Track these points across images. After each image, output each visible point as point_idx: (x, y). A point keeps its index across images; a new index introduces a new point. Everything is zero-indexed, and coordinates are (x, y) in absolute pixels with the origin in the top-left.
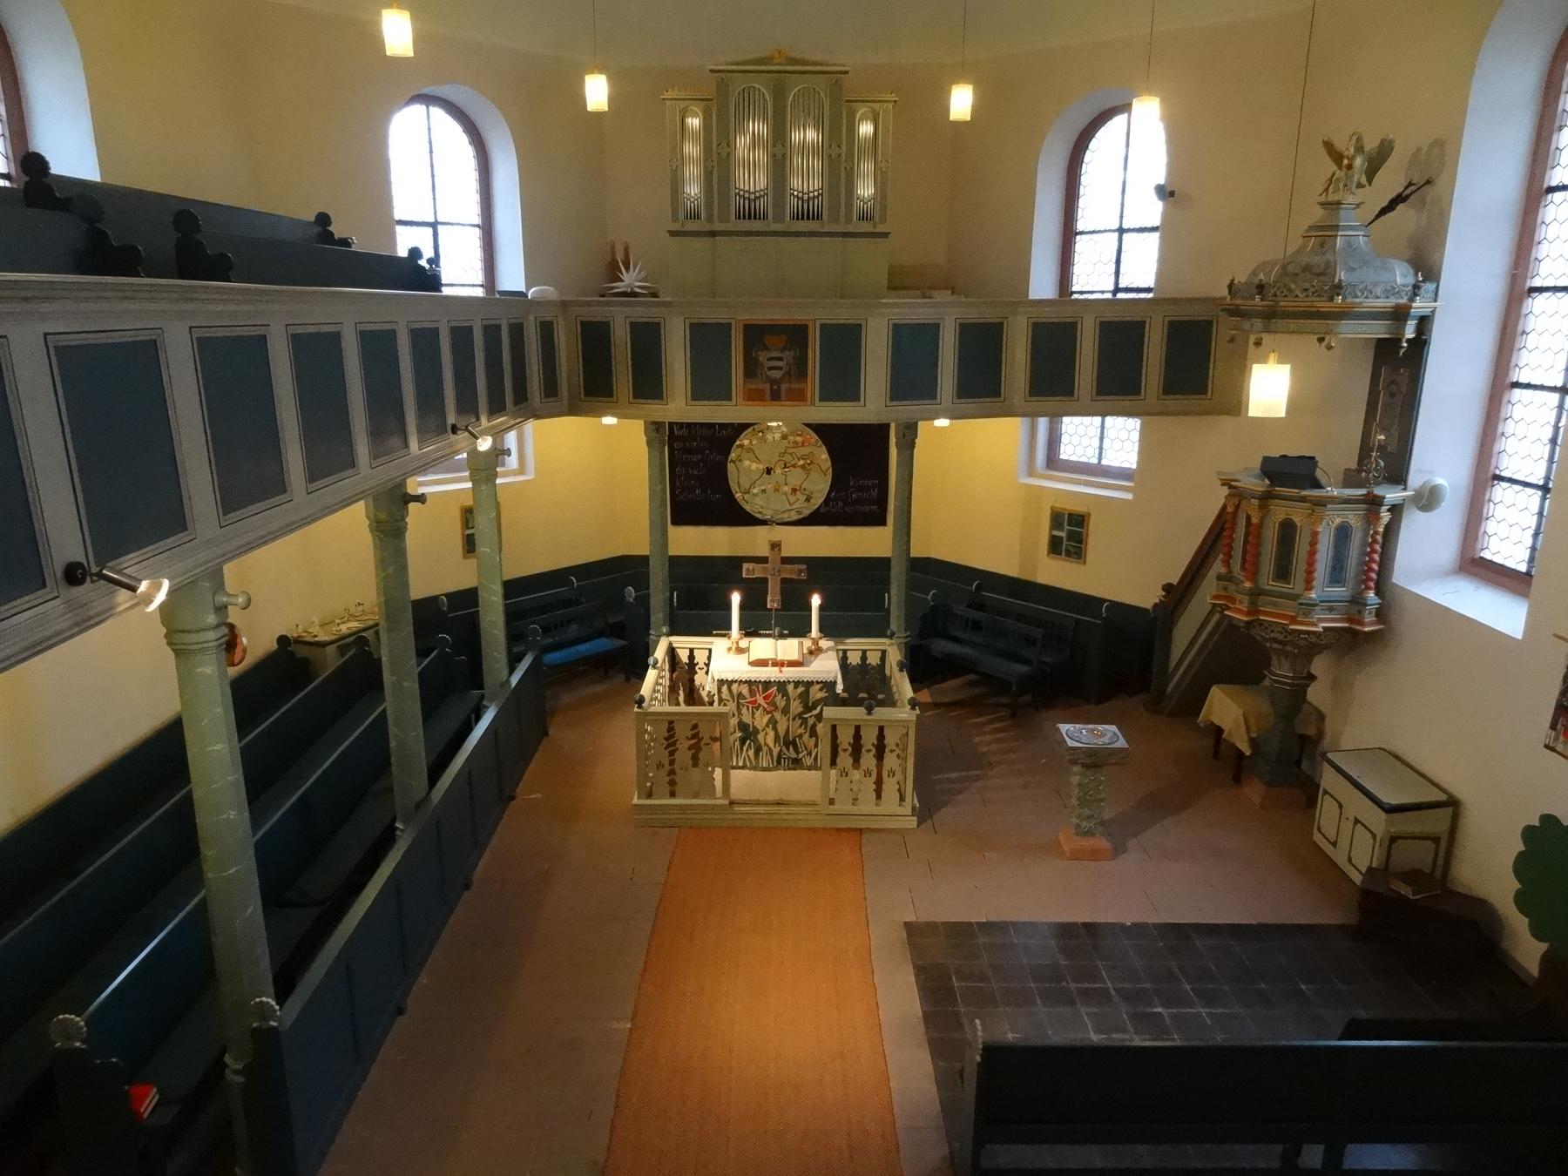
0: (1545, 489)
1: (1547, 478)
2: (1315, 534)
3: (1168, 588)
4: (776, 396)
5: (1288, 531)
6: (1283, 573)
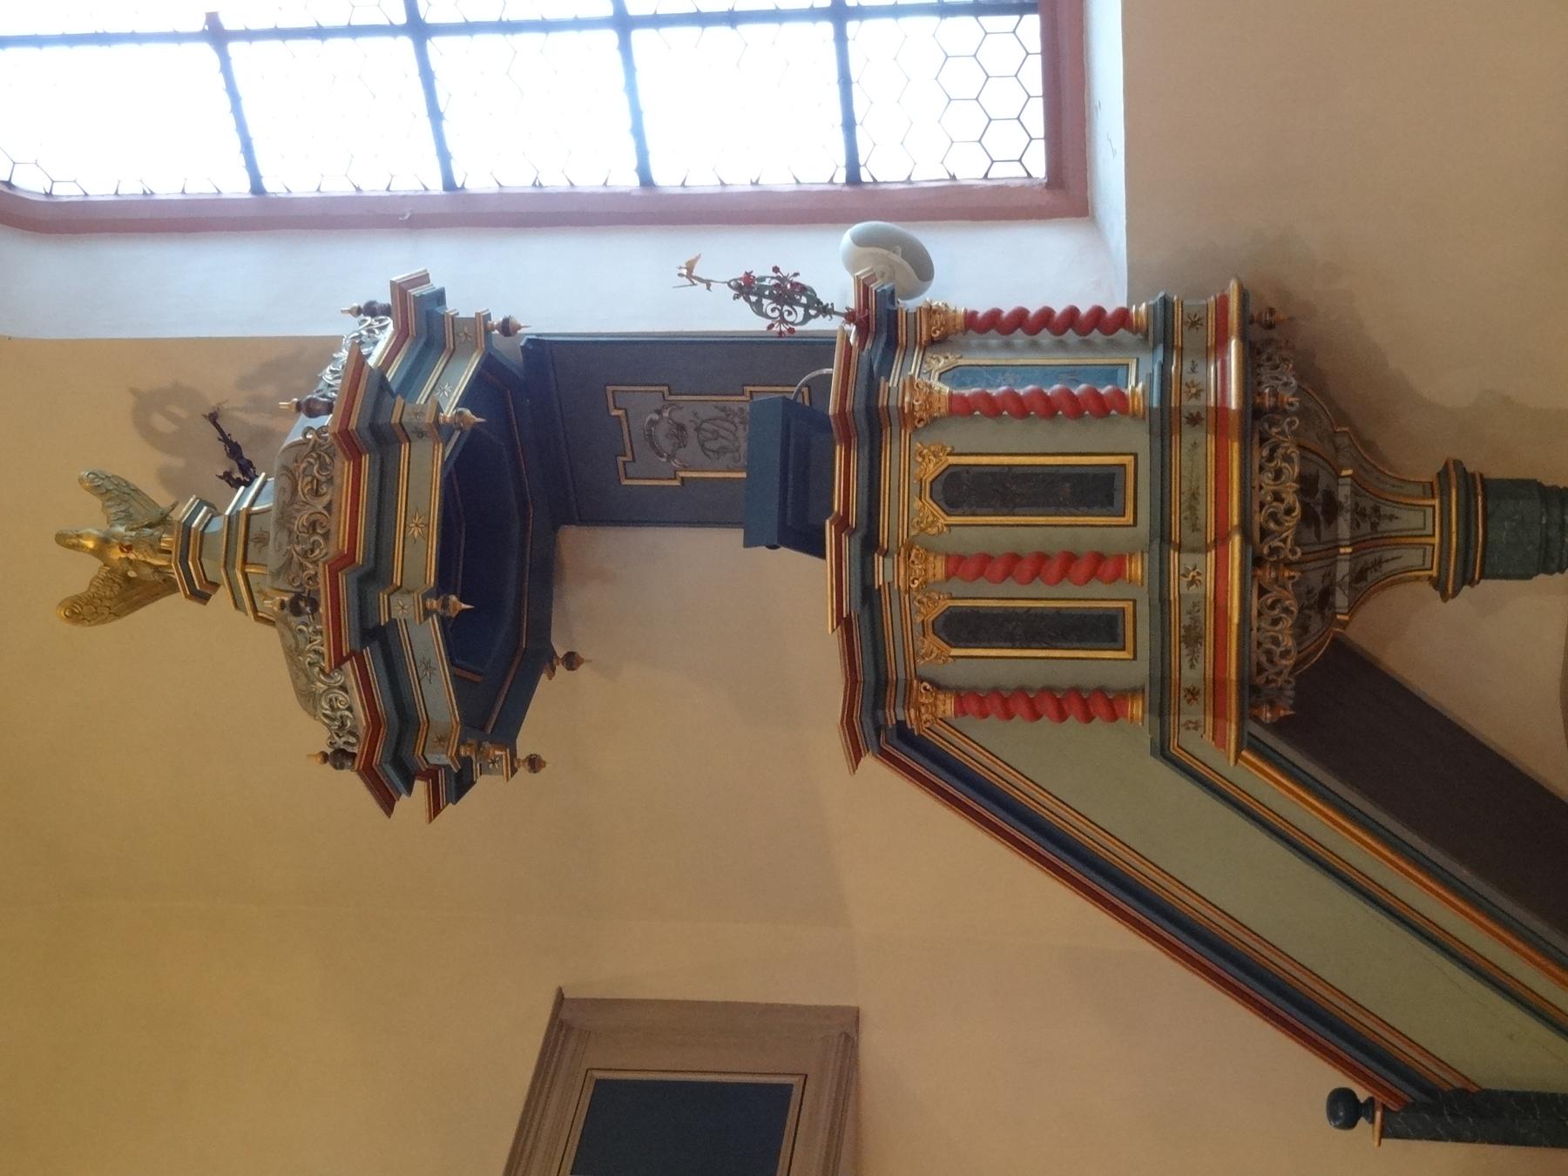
0: (839, 14)
1: (813, 14)
2: (962, 409)
3: (1345, 1110)
5: (963, 490)
6: (1095, 490)
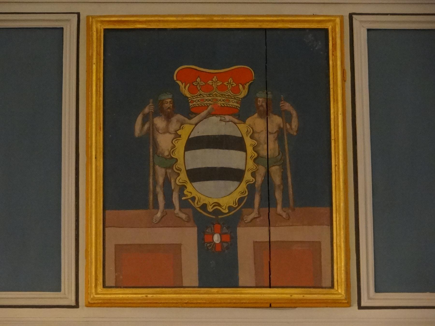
4: (218, 270)
